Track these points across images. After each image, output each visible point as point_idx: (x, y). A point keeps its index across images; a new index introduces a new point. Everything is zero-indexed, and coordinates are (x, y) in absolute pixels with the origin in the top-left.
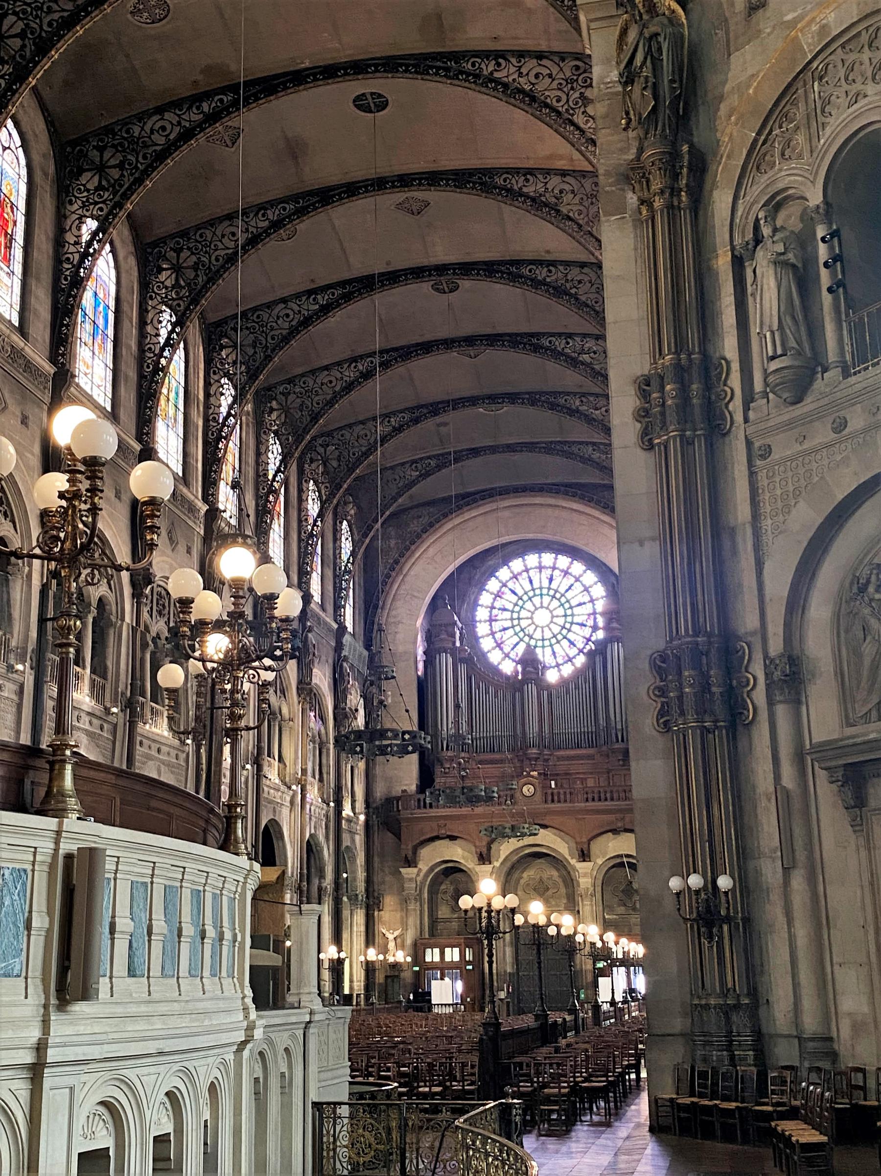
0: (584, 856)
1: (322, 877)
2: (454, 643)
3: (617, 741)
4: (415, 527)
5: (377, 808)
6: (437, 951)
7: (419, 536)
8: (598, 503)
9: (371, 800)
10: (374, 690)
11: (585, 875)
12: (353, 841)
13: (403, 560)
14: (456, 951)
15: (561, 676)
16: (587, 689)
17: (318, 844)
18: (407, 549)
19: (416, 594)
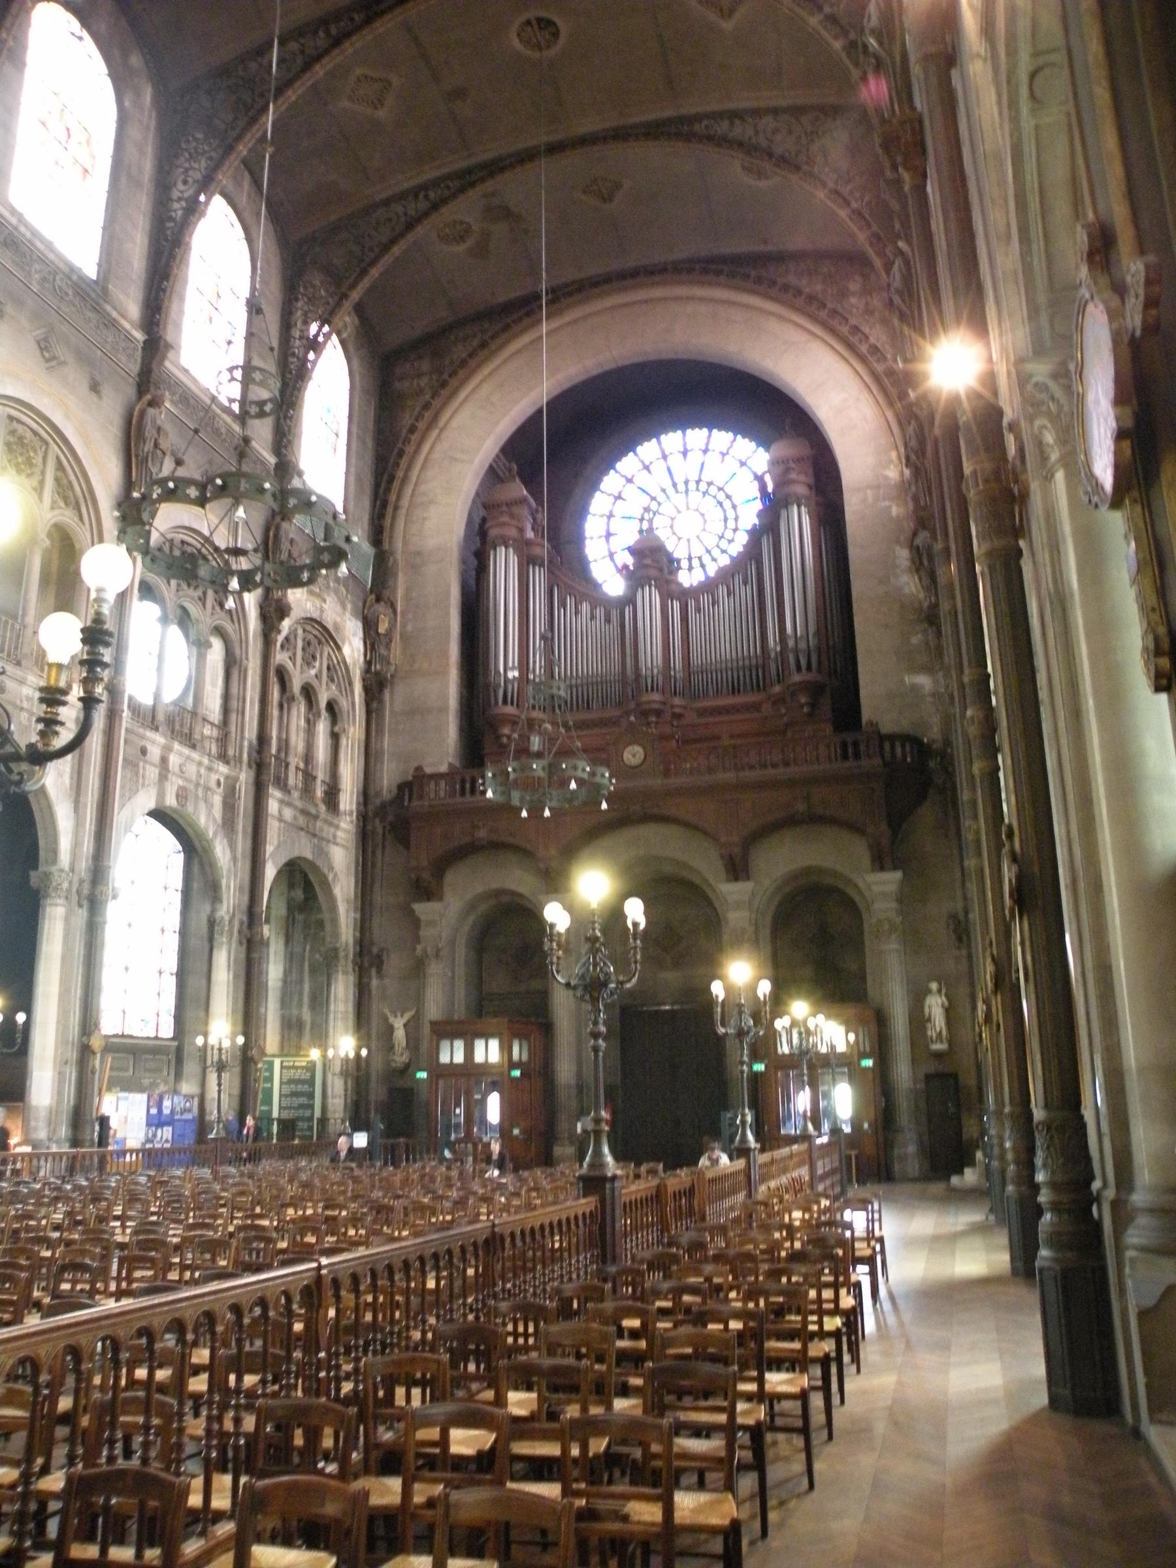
0: (737, 869)
1: (216, 899)
2: (521, 530)
3: (799, 669)
4: (460, 352)
5: (383, 805)
6: (459, 1045)
7: (463, 363)
8: (759, 280)
9: (372, 792)
10: (381, 608)
11: (738, 906)
12: (322, 852)
13: (436, 403)
14: (494, 1044)
15: (707, 577)
16: (746, 594)
17: (201, 835)
18: (444, 384)
19: (459, 455)
